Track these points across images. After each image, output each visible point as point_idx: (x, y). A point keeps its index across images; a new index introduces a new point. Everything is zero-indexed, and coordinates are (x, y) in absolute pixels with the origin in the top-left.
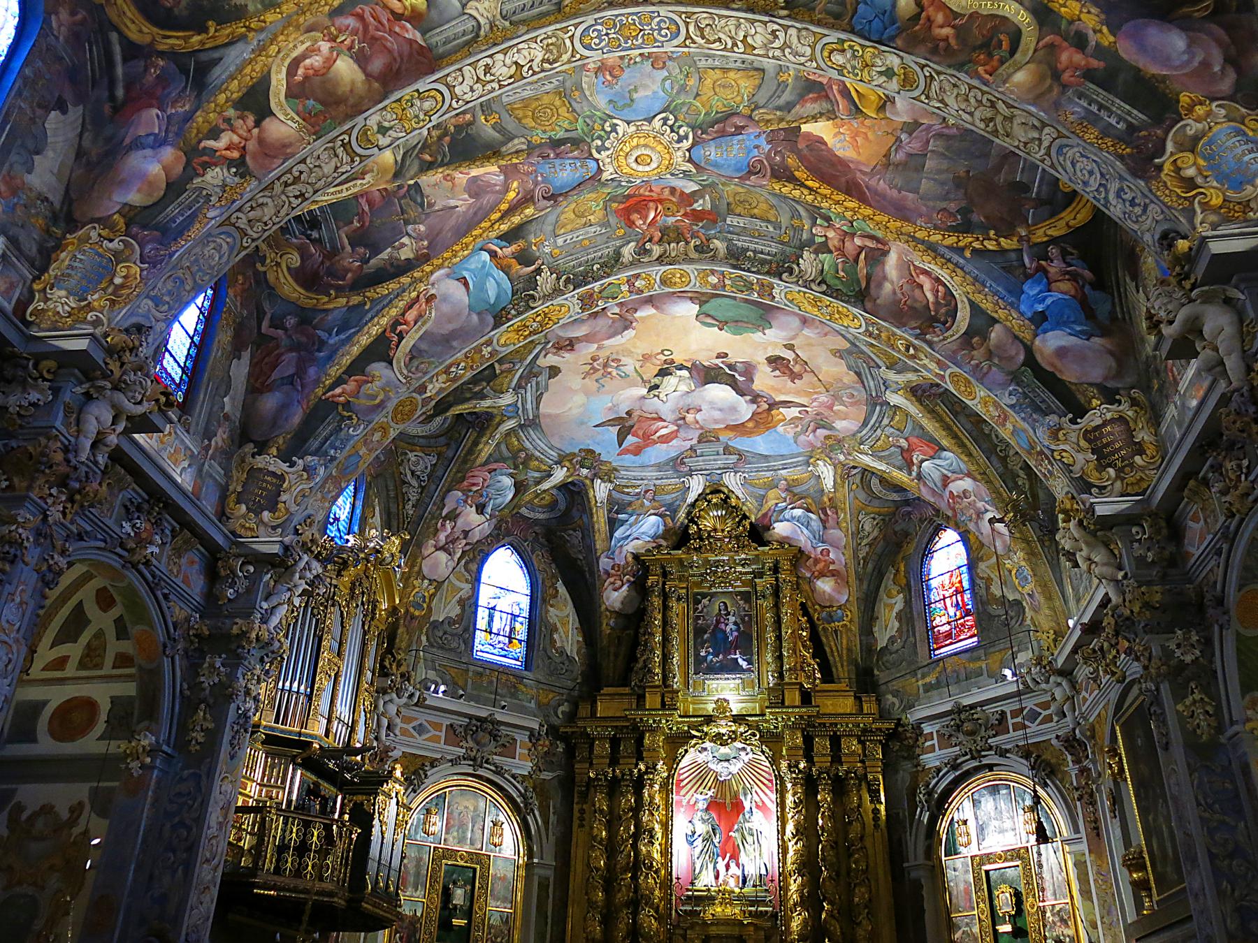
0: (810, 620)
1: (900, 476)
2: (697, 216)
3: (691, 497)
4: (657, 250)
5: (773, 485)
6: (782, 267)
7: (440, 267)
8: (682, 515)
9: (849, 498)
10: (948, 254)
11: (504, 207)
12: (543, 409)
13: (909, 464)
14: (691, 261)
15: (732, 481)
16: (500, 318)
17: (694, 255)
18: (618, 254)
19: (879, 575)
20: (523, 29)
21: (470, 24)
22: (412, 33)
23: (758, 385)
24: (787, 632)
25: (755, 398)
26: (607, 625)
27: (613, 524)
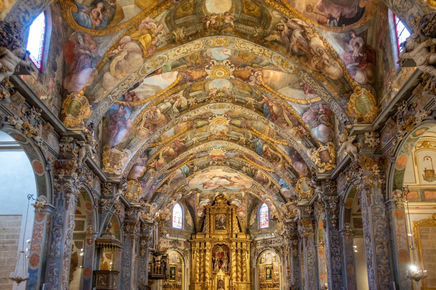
0: (238, 220)
1: (257, 196)
2: (224, 158)
3: (216, 196)
4: (216, 163)
5: (232, 194)
6: (239, 169)
7: (178, 168)
8: (214, 199)
9: (246, 198)
10: (268, 173)
11: (190, 158)
12: (190, 183)
13: (259, 195)
14: (223, 165)
15: (224, 193)
16: (187, 175)
17: (223, 164)
18: (209, 163)
19: (251, 211)
20: (201, 143)
21: (192, 142)
22: (182, 144)
23: (232, 179)
24: (234, 223)
25: (231, 181)
26: (198, 220)
27: (200, 201)
